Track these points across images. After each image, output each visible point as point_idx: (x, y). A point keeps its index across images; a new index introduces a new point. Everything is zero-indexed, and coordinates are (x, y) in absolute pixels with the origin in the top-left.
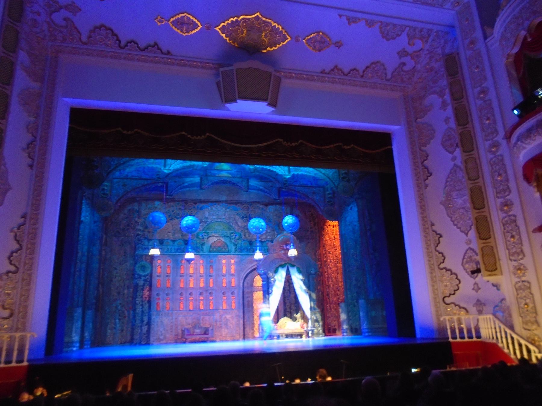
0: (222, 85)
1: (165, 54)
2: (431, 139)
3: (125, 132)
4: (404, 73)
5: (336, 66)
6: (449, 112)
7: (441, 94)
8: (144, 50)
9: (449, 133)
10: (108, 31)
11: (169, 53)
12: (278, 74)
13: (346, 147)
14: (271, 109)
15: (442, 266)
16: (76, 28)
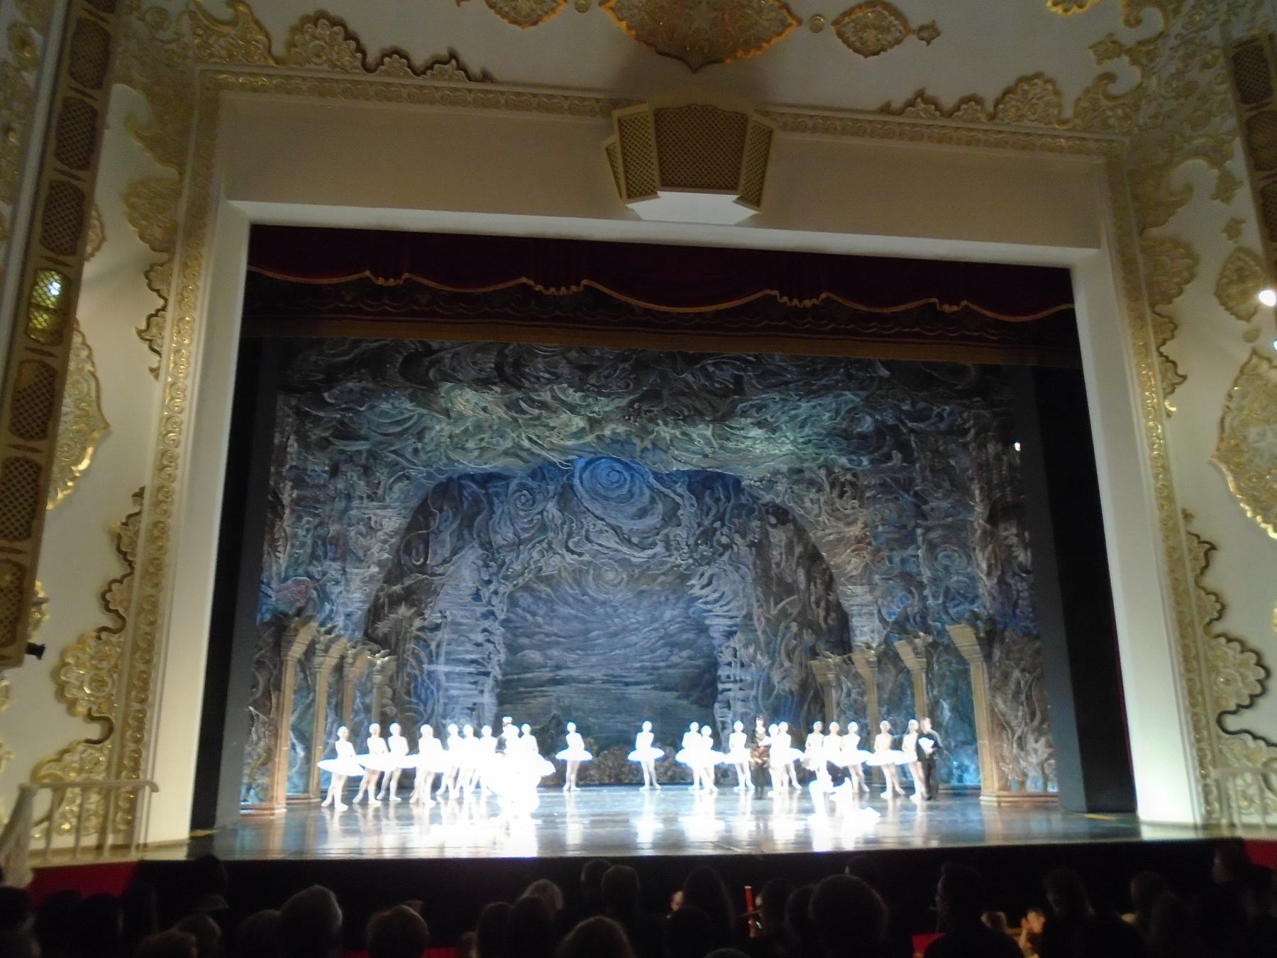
0: (619, 156)
1: (477, 81)
2: (1188, 281)
3: (381, 281)
4: (1110, 104)
5: (920, 94)
6: (1244, 203)
7: (1216, 156)
8: (424, 73)
9: (1240, 264)
10: (335, 29)
11: (486, 77)
12: (766, 122)
13: (947, 308)
14: (748, 212)
15: (1218, 627)
16: (257, 23)
